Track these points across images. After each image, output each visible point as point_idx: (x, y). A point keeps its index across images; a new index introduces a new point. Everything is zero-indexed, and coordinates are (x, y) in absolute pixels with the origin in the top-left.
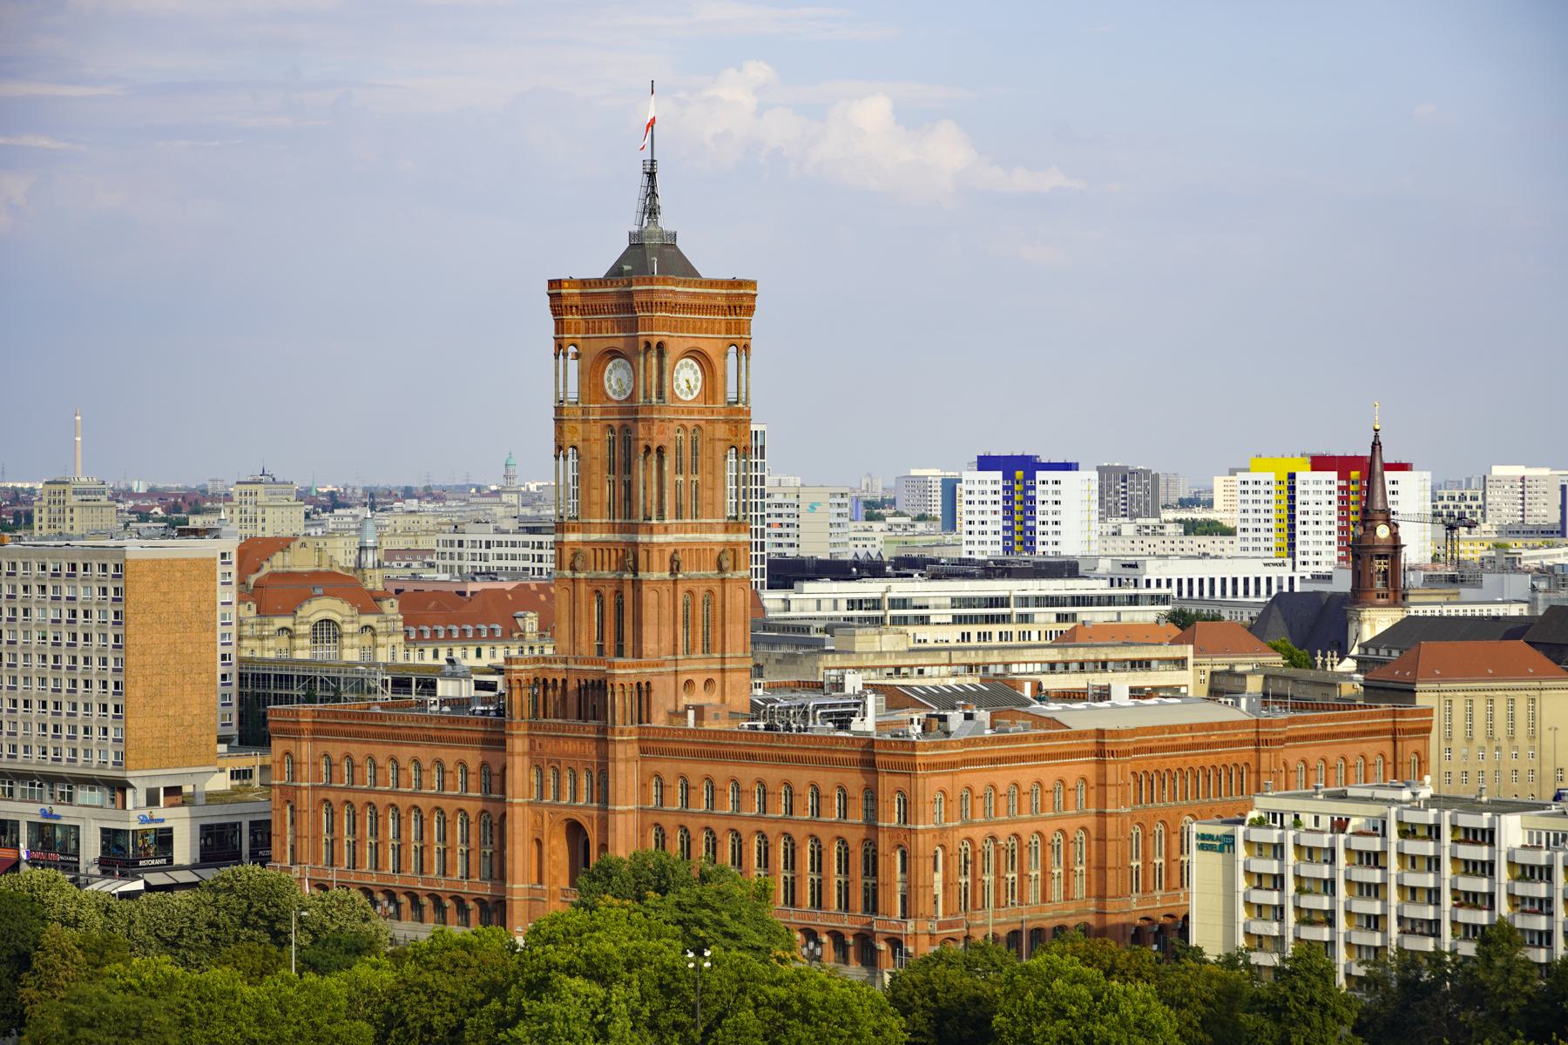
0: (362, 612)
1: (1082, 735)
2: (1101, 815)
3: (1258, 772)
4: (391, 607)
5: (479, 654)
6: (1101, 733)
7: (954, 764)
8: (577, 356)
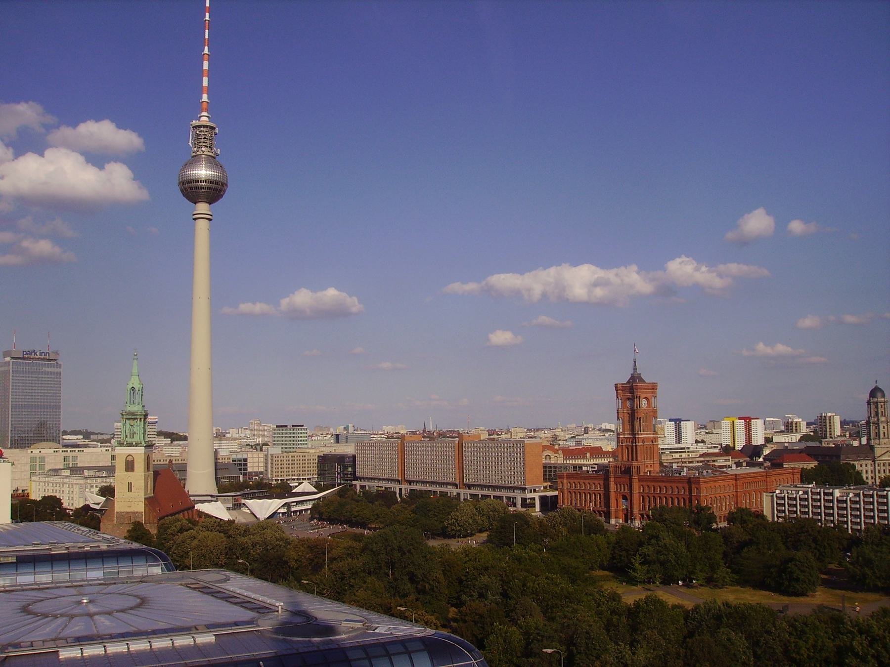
0: (555, 453)
1: (731, 475)
2: (736, 492)
3: (767, 482)
4: (560, 452)
5: (575, 461)
6: (736, 474)
7: (708, 482)
8: (621, 399)
